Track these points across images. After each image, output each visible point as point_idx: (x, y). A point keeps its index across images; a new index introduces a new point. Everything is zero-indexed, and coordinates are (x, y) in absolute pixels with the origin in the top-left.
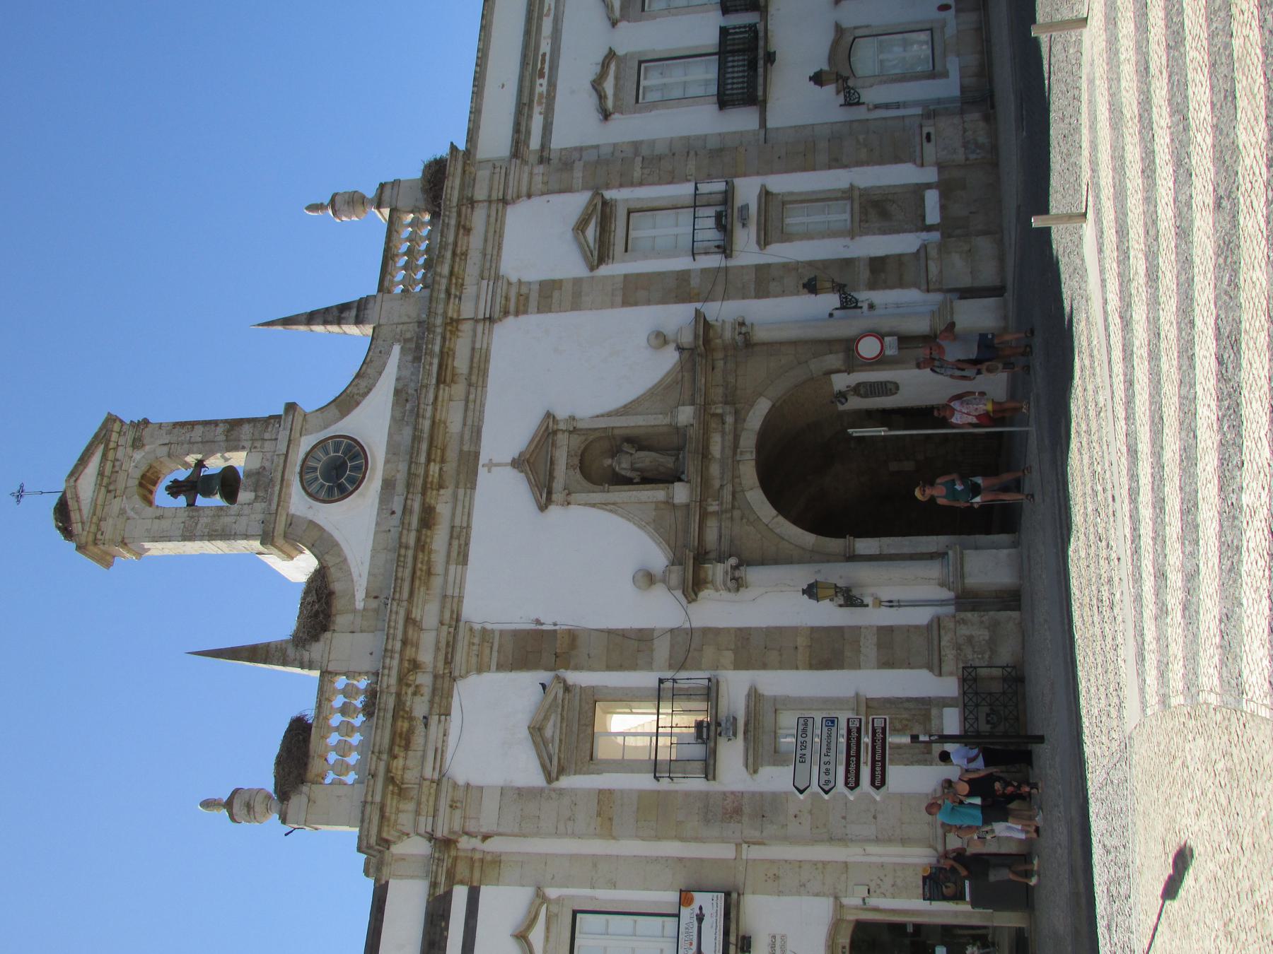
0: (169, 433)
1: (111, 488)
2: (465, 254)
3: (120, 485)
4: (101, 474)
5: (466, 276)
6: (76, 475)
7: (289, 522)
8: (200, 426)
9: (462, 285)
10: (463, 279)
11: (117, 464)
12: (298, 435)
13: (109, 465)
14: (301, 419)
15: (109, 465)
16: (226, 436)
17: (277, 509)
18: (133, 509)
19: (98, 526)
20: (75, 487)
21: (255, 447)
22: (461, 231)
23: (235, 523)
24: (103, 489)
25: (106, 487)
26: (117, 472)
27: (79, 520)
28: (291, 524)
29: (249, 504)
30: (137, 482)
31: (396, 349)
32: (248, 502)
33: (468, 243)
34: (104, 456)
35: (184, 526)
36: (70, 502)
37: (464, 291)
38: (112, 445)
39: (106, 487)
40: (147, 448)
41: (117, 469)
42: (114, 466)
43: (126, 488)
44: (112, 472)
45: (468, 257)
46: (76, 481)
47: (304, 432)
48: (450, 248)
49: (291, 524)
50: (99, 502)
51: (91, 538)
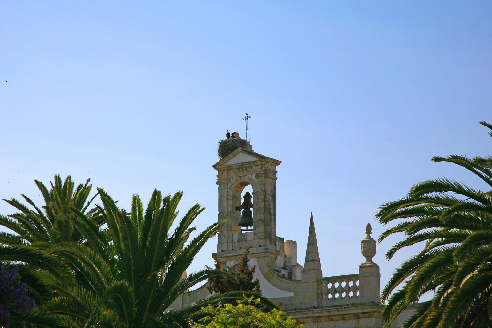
0: (262, 190)
1: (240, 169)
2: (332, 320)
3: (242, 174)
4: (243, 164)
5: (323, 323)
6: (243, 152)
7: (223, 263)
8: (263, 205)
9: (318, 322)
10: (320, 321)
11: (250, 168)
12: (257, 256)
13: (249, 165)
14: (263, 256)
15: (249, 165)
16: (259, 220)
17: (224, 257)
18: (232, 184)
19: (225, 170)
20: (239, 153)
21: (255, 235)
22: (341, 317)
23: (224, 237)
24: (238, 167)
25: (240, 167)
26: (247, 170)
27: (224, 162)
28: (223, 264)
29: (232, 241)
30: (242, 181)
31: (292, 294)
32: (233, 239)
33: (338, 320)
34: (250, 163)
35: (223, 213)
36: (231, 155)
37: (314, 323)
38: (256, 164)
39: (240, 167)
40: (257, 180)
41: (248, 169)
42: (249, 167)
43: (240, 177)
44: (246, 167)
45: (331, 322)
46: (241, 152)
47: (258, 258)
48: (329, 314)
49: (223, 264)
50: (234, 167)
51: (220, 169)
